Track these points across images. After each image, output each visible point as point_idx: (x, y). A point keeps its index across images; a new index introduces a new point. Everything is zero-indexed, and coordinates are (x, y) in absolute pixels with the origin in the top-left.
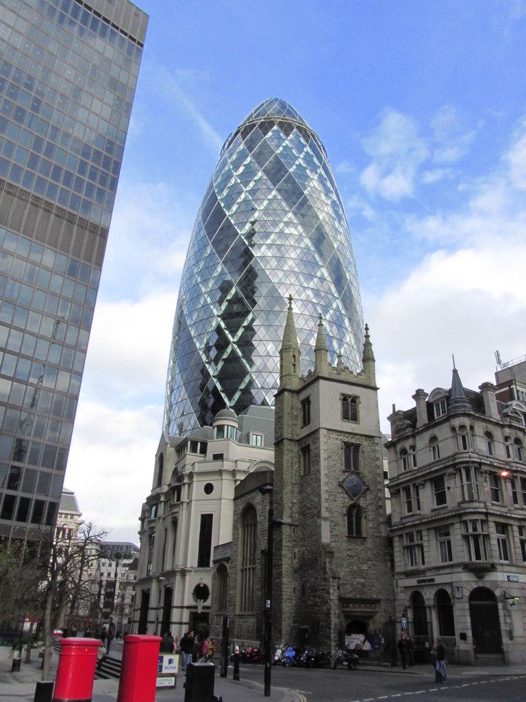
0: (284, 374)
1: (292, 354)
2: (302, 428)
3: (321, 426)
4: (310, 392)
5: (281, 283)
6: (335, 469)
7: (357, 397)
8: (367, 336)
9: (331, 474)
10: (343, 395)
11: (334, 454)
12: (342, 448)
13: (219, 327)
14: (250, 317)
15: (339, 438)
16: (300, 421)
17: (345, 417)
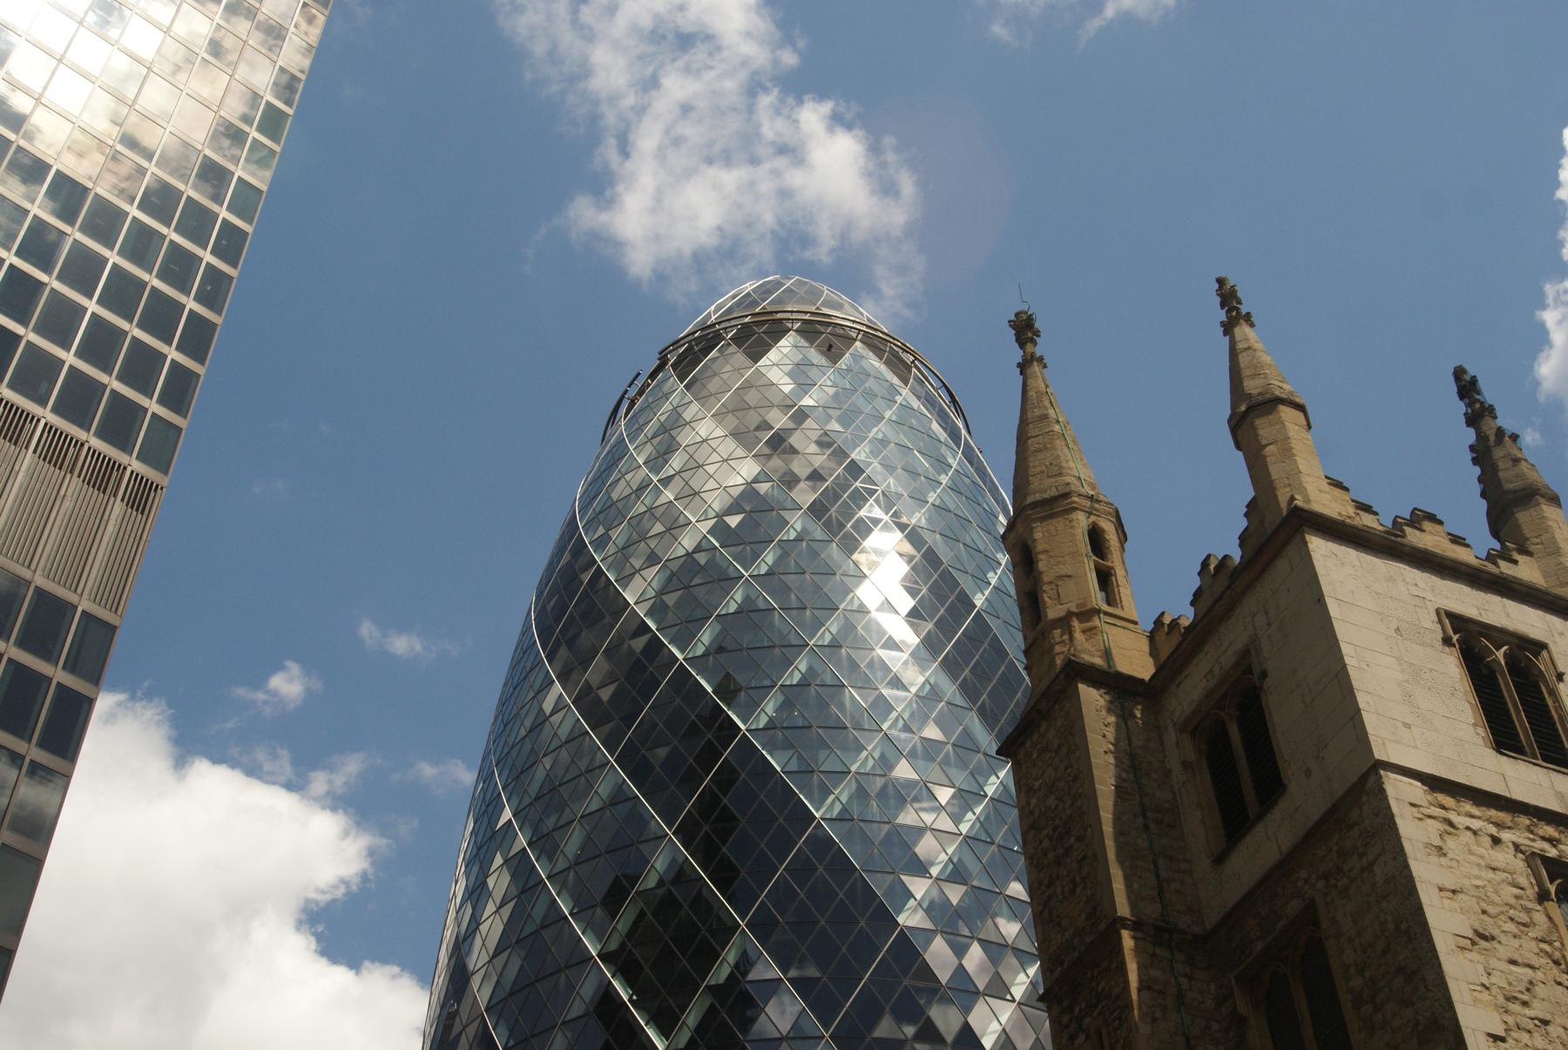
0: (1053, 612)
1: (1082, 521)
2: (1219, 859)
3: (1379, 754)
4: (1238, 646)
5: (844, 818)
6: (1538, 1010)
7: (1539, 647)
8: (1478, 414)
9: (1525, 1037)
10: (1457, 622)
11: (1510, 927)
12: (1543, 897)
13: (607, 996)
14: (731, 955)
15: (1506, 836)
16: (1198, 824)
17: (1504, 740)
